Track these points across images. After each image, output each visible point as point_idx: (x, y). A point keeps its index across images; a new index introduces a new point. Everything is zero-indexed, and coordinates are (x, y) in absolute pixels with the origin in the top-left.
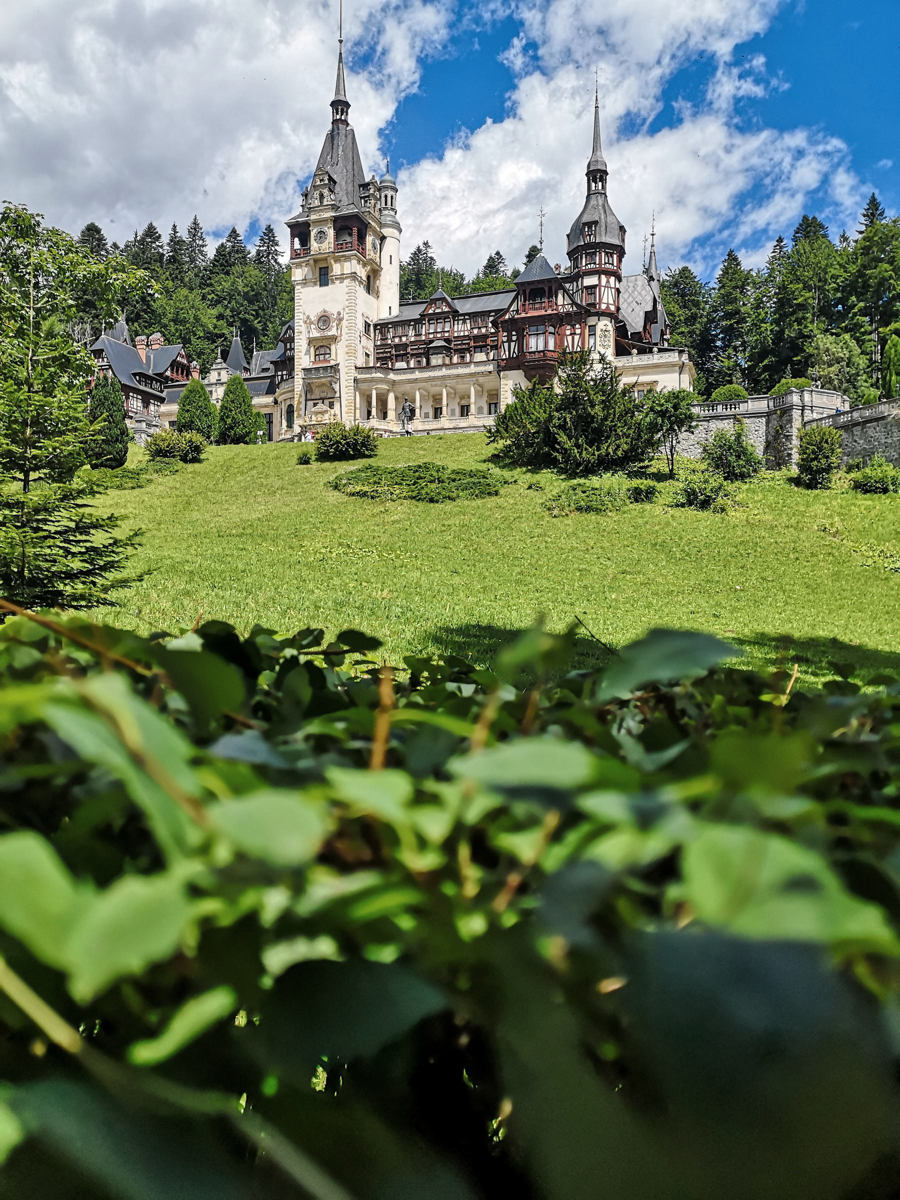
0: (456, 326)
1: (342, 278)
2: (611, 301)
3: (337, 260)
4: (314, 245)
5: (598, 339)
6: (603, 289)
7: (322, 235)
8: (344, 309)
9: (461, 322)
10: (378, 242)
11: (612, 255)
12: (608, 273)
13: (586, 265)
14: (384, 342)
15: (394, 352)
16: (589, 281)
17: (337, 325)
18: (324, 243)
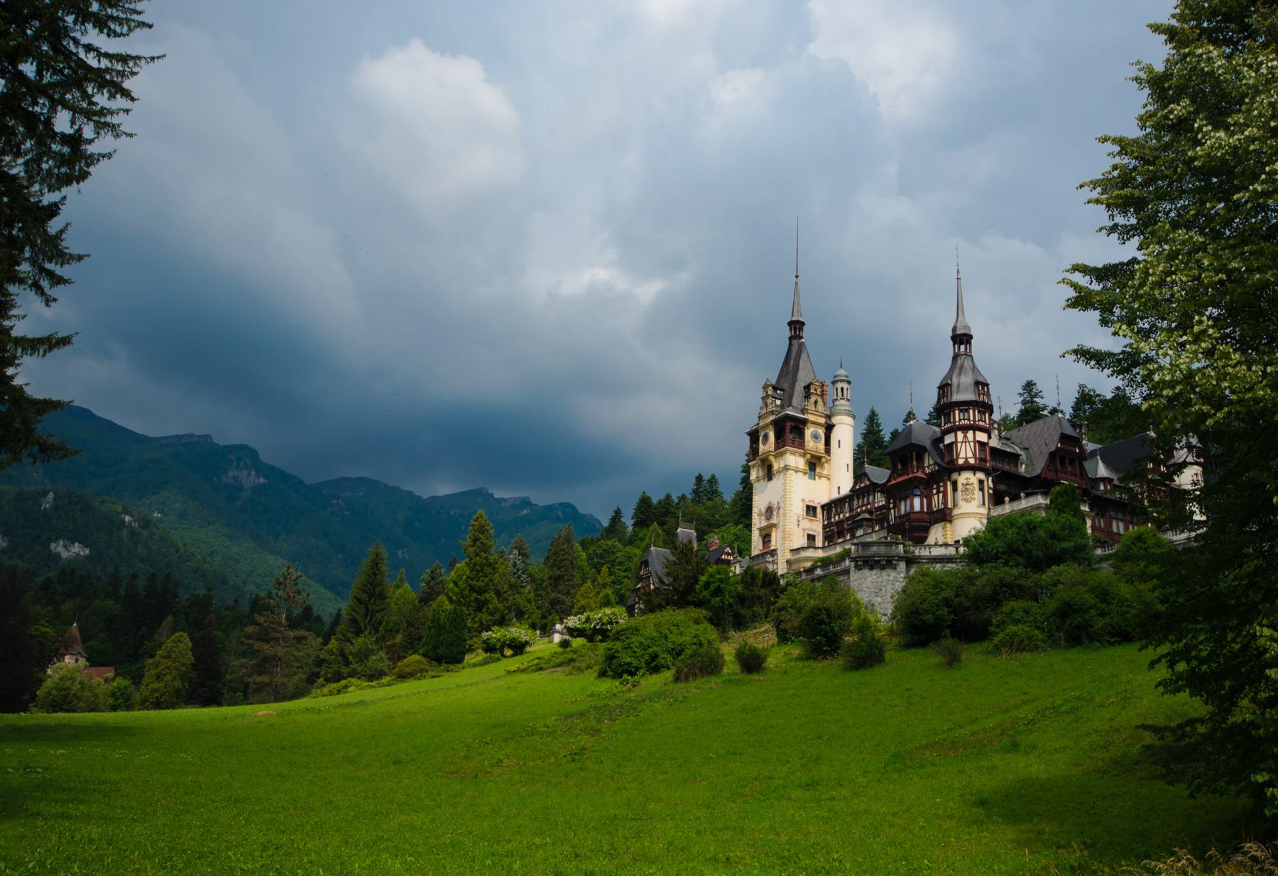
1: (779, 472)
2: (970, 454)
3: (776, 456)
4: (761, 446)
5: (959, 493)
7: (766, 437)
10: (821, 432)
11: (967, 411)
12: (965, 429)
16: (949, 439)
18: (767, 446)
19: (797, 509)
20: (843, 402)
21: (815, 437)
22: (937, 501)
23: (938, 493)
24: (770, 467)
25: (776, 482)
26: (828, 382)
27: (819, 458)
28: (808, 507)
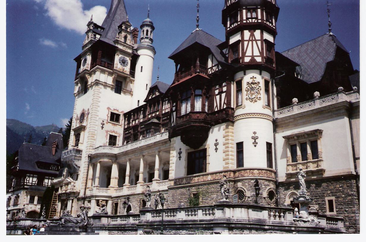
0: (164, 107)
2: (257, 53)
3: (90, 74)
5: (244, 92)
6: (246, 43)
8: (90, 106)
9: (167, 102)
10: (128, 60)
11: (255, 10)
12: (252, 28)
13: (230, 25)
14: (128, 126)
15: (132, 132)
17: (87, 119)
19: (105, 115)
20: (147, 40)
21: (123, 62)
22: (219, 101)
23: (220, 93)
24: (87, 82)
25: (90, 92)
26: (139, 29)
27: (125, 78)
28: (113, 114)
